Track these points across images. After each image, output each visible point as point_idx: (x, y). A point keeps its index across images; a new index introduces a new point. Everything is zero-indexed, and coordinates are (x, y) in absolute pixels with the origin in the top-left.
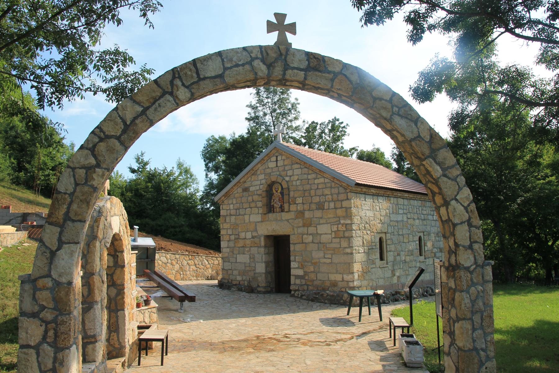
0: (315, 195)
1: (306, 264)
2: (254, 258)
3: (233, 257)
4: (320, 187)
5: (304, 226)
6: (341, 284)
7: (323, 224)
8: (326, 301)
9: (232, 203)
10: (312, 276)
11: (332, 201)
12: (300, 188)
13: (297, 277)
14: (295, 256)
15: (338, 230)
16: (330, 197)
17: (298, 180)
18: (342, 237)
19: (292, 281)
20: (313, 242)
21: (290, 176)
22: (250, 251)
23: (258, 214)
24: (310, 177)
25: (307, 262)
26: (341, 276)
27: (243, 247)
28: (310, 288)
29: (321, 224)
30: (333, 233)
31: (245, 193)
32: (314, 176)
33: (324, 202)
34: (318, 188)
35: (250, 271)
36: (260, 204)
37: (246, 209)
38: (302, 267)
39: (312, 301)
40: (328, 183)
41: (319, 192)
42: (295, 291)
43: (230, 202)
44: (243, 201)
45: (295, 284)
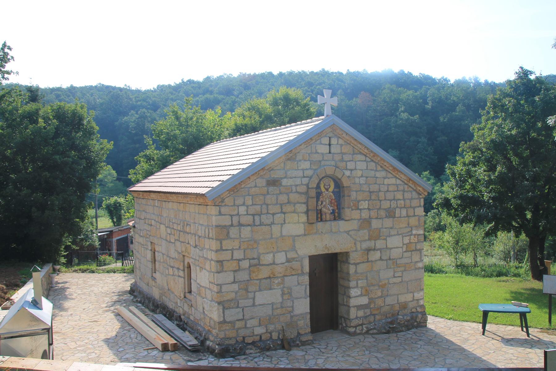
0: (385, 199)
1: (372, 288)
2: (290, 294)
3: (247, 298)
4: (391, 189)
5: (370, 239)
6: (411, 305)
7: (394, 235)
8: (403, 328)
9: (244, 204)
10: (380, 302)
11: (404, 207)
12: (365, 188)
13: (359, 307)
14: (357, 280)
15: (410, 243)
16: (402, 202)
17: (362, 176)
18: (413, 251)
19: (353, 313)
20: (381, 259)
21: (351, 170)
22: (283, 282)
23: (298, 223)
24: (378, 174)
25: (374, 286)
26: (411, 295)
27: (270, 278)
28: (378, 317)
29: (392, 236)
30: (405, 246)
31: (271, 189)
32: (383, 174)
33: (395, 209)
34: (388, 191)
35: (284, 314)
36: (303, 208)
37: (273, 214)
38: (366, 292)
39: (388, 332)
40: (400, 184)
41: (390, 196)
42: (356, 327)
43: (239, 201)
44: (269, 202)
45: (357, 318)
